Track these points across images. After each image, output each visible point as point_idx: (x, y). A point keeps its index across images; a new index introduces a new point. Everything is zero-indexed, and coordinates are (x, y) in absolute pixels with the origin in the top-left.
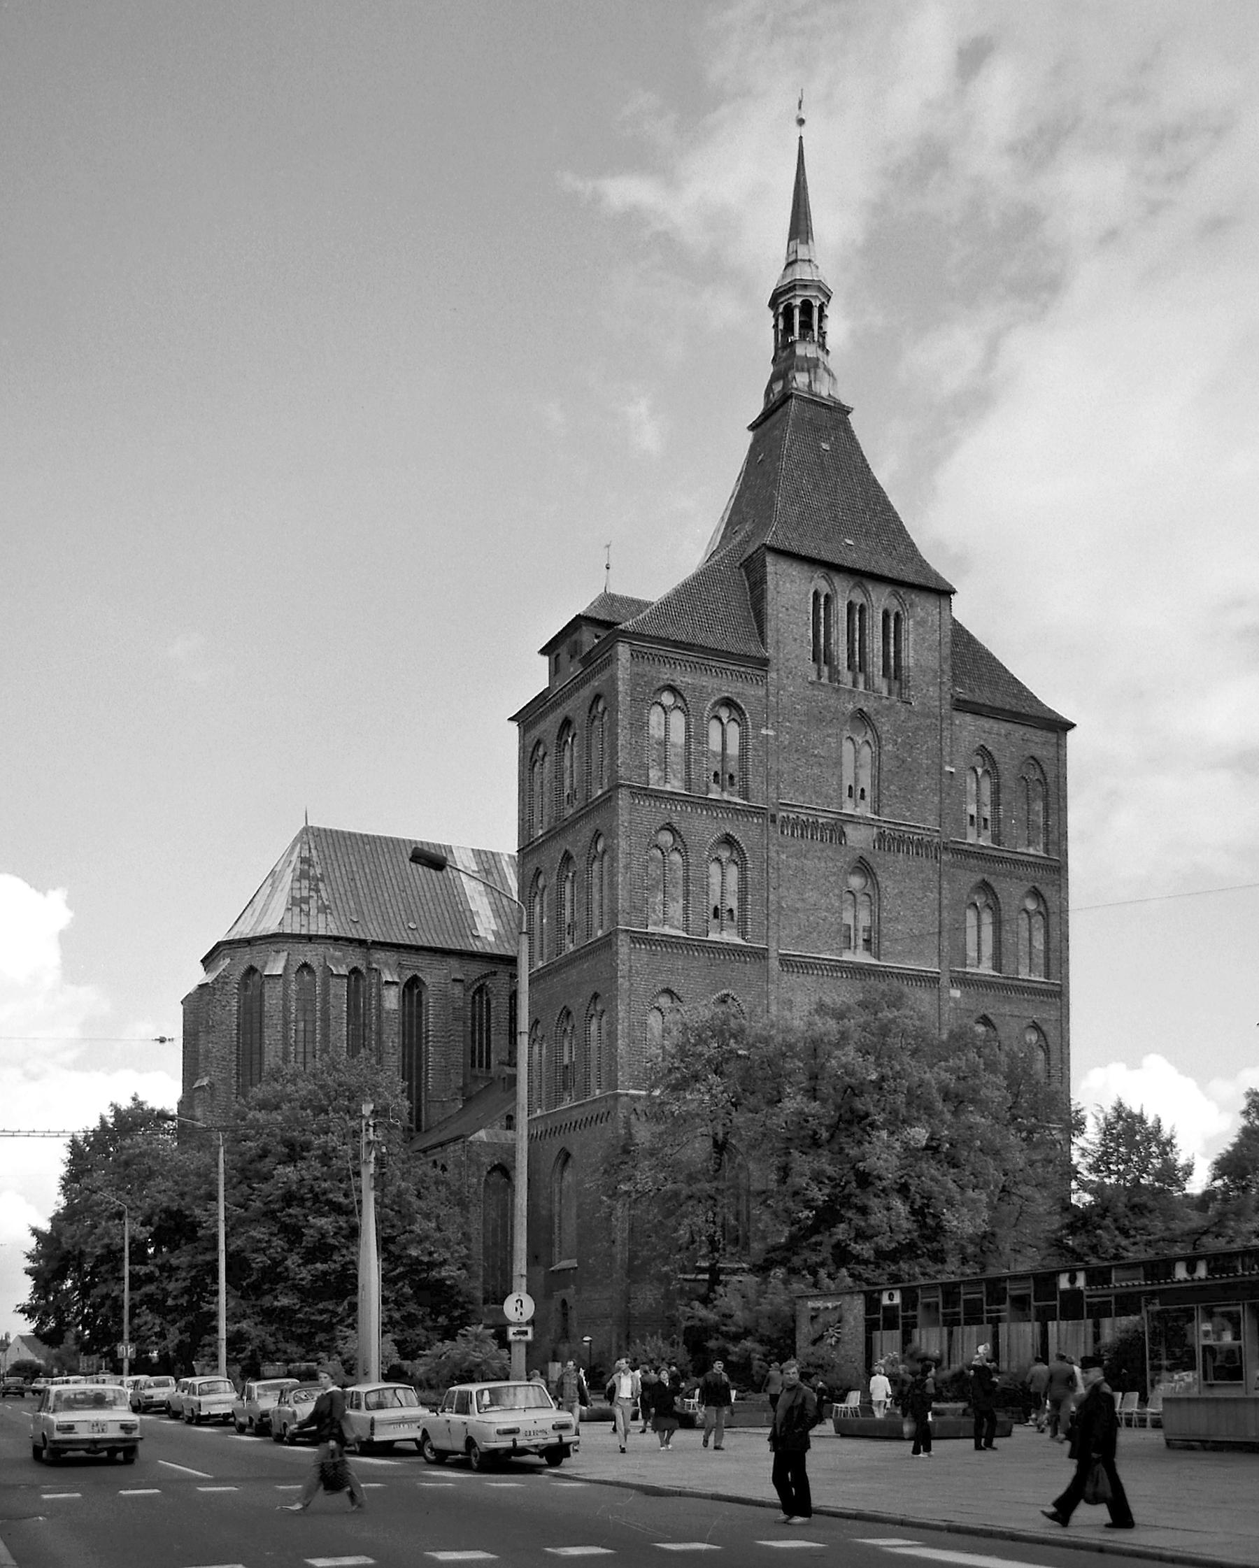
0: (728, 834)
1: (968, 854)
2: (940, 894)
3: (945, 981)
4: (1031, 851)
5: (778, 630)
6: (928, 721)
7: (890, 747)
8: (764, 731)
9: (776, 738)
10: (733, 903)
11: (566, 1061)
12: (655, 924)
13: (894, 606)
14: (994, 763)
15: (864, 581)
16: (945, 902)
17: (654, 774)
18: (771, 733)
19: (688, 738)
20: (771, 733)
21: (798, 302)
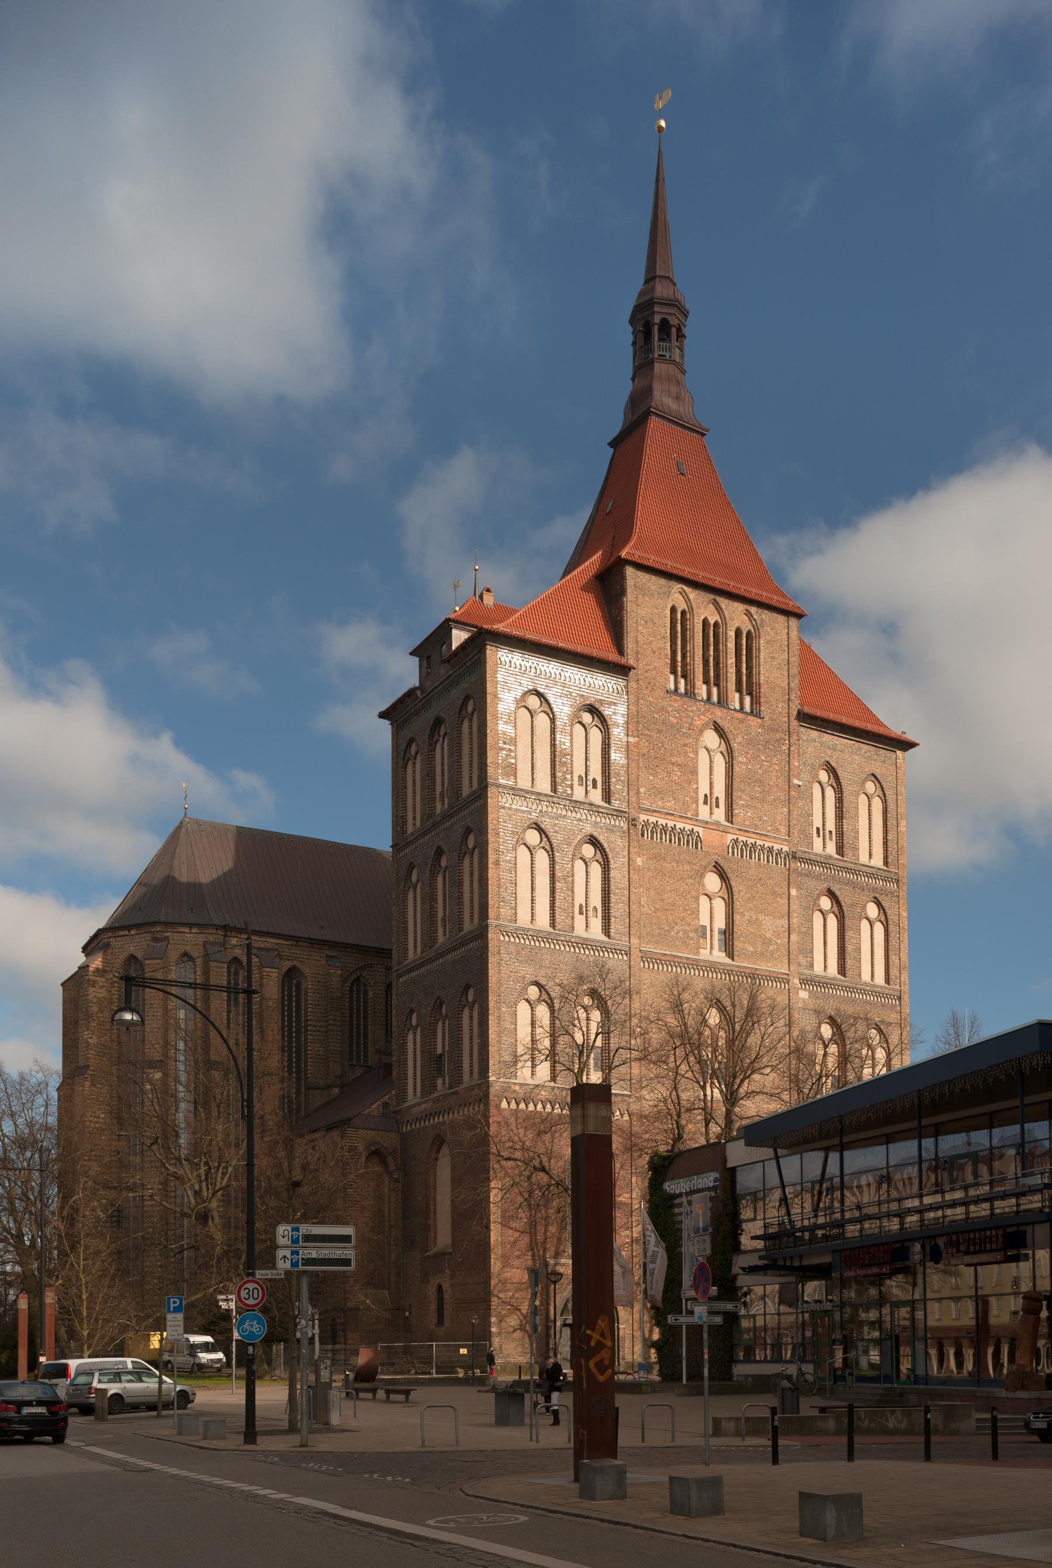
0: (592, 836)
6: (778, 736)
11: (439, 1051)
13: (746, 627)
21: (657, 319)
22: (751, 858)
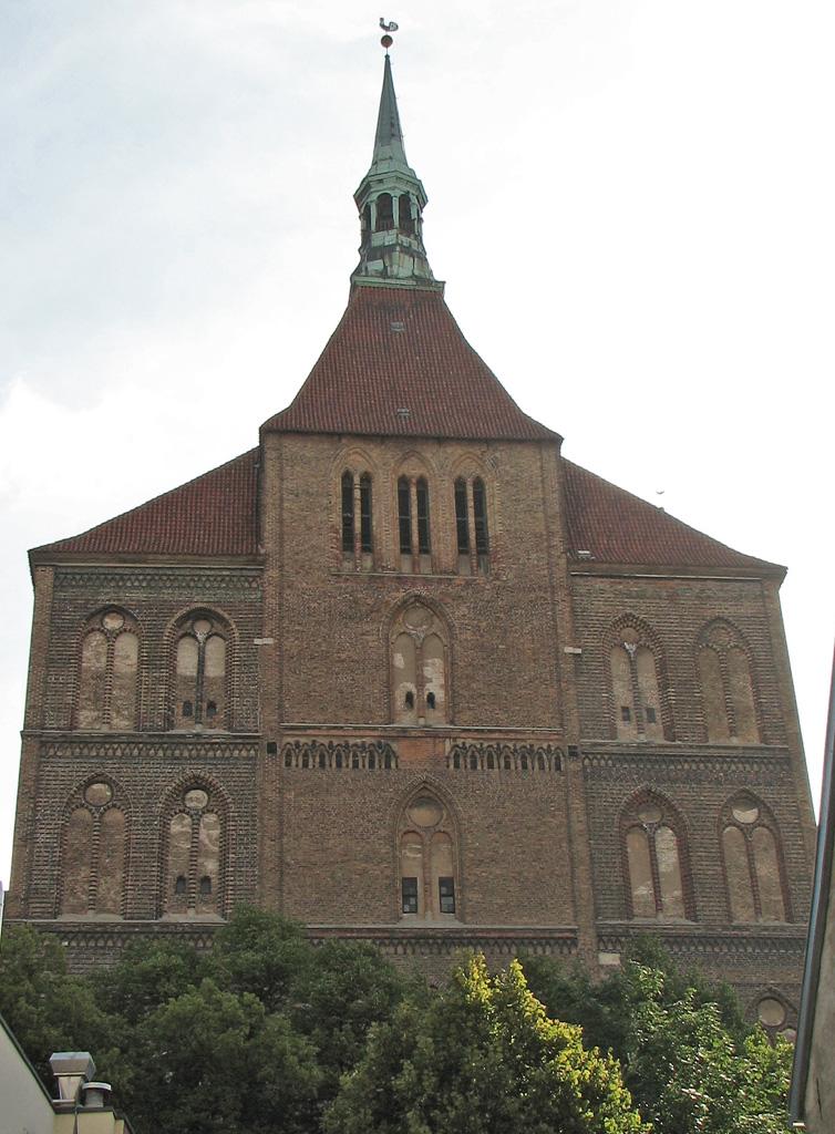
1: (623, 757)
2: (568, 816)
3: (587, 939)
4: (735, 741)
5: (281, 522)
6: (533, 595)
7: (468, 635)
8: (257, 641)
9: (279, 647)
10: (211, 866)
12: (74, 910)
14: (652, 635)
15: (418, 448)
16: (578, 827)
17: (86, 717)
18: (270, 641)
19: (141, 662)
20: (270, 641)
22: (491, 766)
